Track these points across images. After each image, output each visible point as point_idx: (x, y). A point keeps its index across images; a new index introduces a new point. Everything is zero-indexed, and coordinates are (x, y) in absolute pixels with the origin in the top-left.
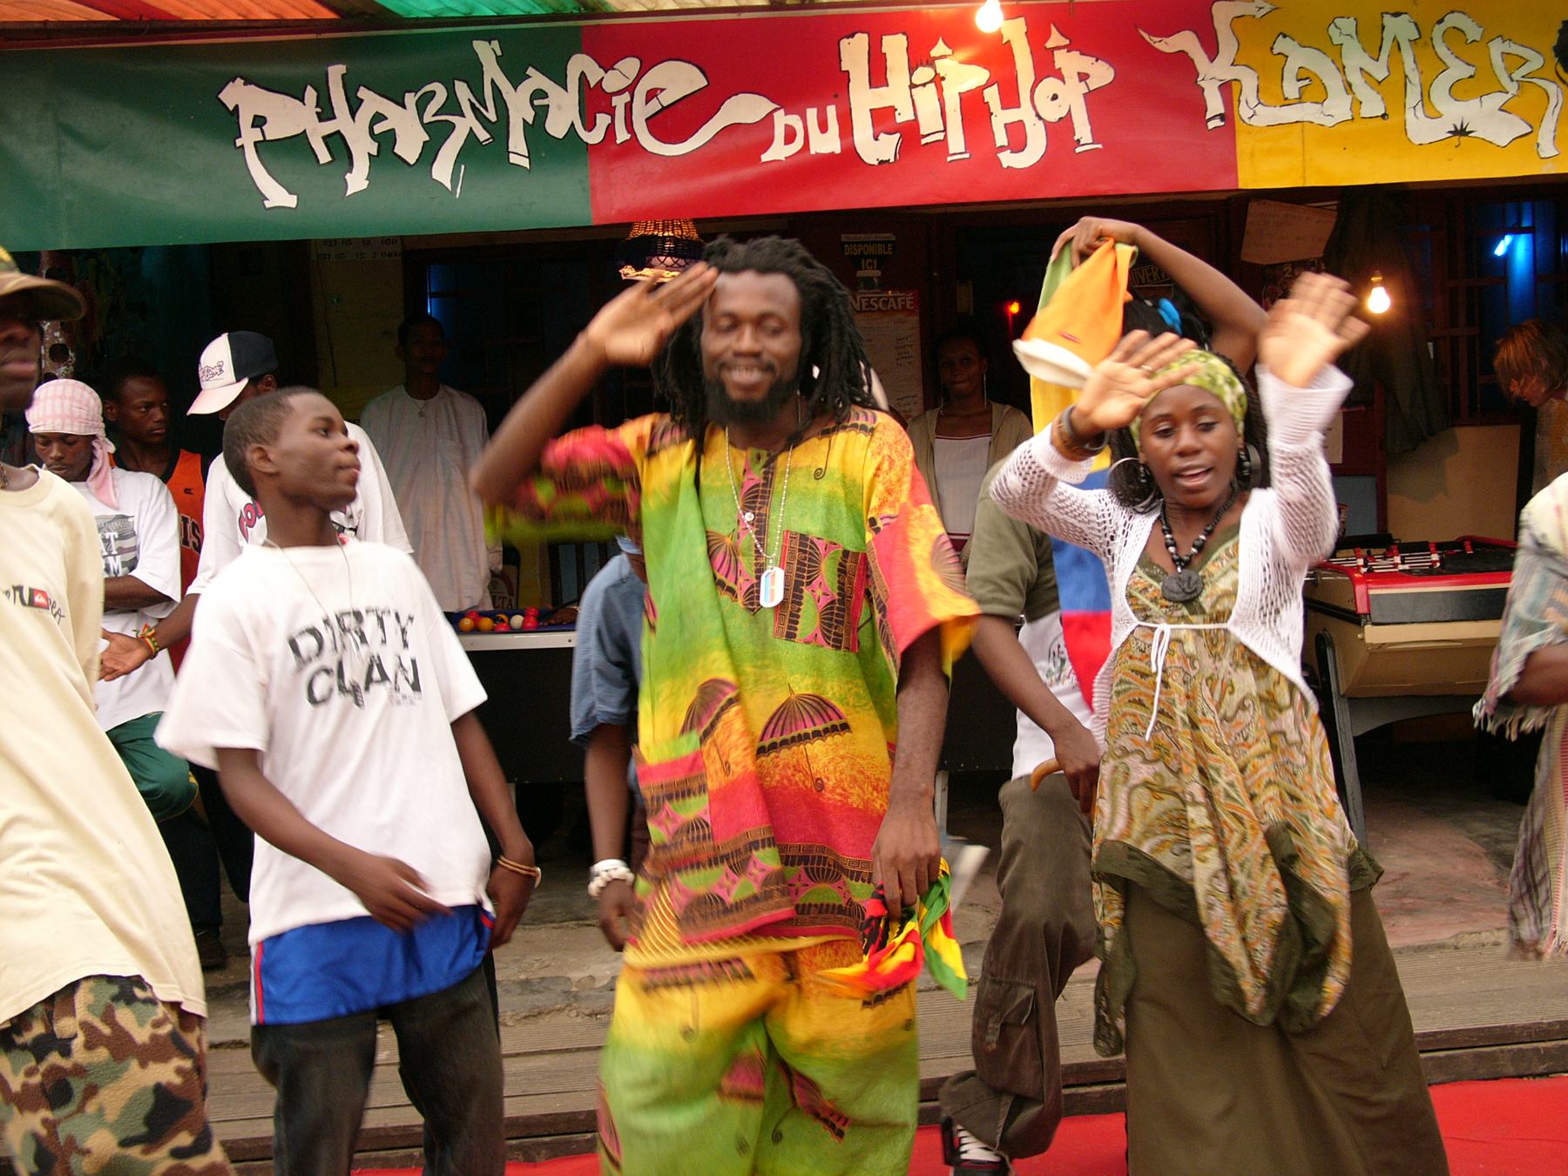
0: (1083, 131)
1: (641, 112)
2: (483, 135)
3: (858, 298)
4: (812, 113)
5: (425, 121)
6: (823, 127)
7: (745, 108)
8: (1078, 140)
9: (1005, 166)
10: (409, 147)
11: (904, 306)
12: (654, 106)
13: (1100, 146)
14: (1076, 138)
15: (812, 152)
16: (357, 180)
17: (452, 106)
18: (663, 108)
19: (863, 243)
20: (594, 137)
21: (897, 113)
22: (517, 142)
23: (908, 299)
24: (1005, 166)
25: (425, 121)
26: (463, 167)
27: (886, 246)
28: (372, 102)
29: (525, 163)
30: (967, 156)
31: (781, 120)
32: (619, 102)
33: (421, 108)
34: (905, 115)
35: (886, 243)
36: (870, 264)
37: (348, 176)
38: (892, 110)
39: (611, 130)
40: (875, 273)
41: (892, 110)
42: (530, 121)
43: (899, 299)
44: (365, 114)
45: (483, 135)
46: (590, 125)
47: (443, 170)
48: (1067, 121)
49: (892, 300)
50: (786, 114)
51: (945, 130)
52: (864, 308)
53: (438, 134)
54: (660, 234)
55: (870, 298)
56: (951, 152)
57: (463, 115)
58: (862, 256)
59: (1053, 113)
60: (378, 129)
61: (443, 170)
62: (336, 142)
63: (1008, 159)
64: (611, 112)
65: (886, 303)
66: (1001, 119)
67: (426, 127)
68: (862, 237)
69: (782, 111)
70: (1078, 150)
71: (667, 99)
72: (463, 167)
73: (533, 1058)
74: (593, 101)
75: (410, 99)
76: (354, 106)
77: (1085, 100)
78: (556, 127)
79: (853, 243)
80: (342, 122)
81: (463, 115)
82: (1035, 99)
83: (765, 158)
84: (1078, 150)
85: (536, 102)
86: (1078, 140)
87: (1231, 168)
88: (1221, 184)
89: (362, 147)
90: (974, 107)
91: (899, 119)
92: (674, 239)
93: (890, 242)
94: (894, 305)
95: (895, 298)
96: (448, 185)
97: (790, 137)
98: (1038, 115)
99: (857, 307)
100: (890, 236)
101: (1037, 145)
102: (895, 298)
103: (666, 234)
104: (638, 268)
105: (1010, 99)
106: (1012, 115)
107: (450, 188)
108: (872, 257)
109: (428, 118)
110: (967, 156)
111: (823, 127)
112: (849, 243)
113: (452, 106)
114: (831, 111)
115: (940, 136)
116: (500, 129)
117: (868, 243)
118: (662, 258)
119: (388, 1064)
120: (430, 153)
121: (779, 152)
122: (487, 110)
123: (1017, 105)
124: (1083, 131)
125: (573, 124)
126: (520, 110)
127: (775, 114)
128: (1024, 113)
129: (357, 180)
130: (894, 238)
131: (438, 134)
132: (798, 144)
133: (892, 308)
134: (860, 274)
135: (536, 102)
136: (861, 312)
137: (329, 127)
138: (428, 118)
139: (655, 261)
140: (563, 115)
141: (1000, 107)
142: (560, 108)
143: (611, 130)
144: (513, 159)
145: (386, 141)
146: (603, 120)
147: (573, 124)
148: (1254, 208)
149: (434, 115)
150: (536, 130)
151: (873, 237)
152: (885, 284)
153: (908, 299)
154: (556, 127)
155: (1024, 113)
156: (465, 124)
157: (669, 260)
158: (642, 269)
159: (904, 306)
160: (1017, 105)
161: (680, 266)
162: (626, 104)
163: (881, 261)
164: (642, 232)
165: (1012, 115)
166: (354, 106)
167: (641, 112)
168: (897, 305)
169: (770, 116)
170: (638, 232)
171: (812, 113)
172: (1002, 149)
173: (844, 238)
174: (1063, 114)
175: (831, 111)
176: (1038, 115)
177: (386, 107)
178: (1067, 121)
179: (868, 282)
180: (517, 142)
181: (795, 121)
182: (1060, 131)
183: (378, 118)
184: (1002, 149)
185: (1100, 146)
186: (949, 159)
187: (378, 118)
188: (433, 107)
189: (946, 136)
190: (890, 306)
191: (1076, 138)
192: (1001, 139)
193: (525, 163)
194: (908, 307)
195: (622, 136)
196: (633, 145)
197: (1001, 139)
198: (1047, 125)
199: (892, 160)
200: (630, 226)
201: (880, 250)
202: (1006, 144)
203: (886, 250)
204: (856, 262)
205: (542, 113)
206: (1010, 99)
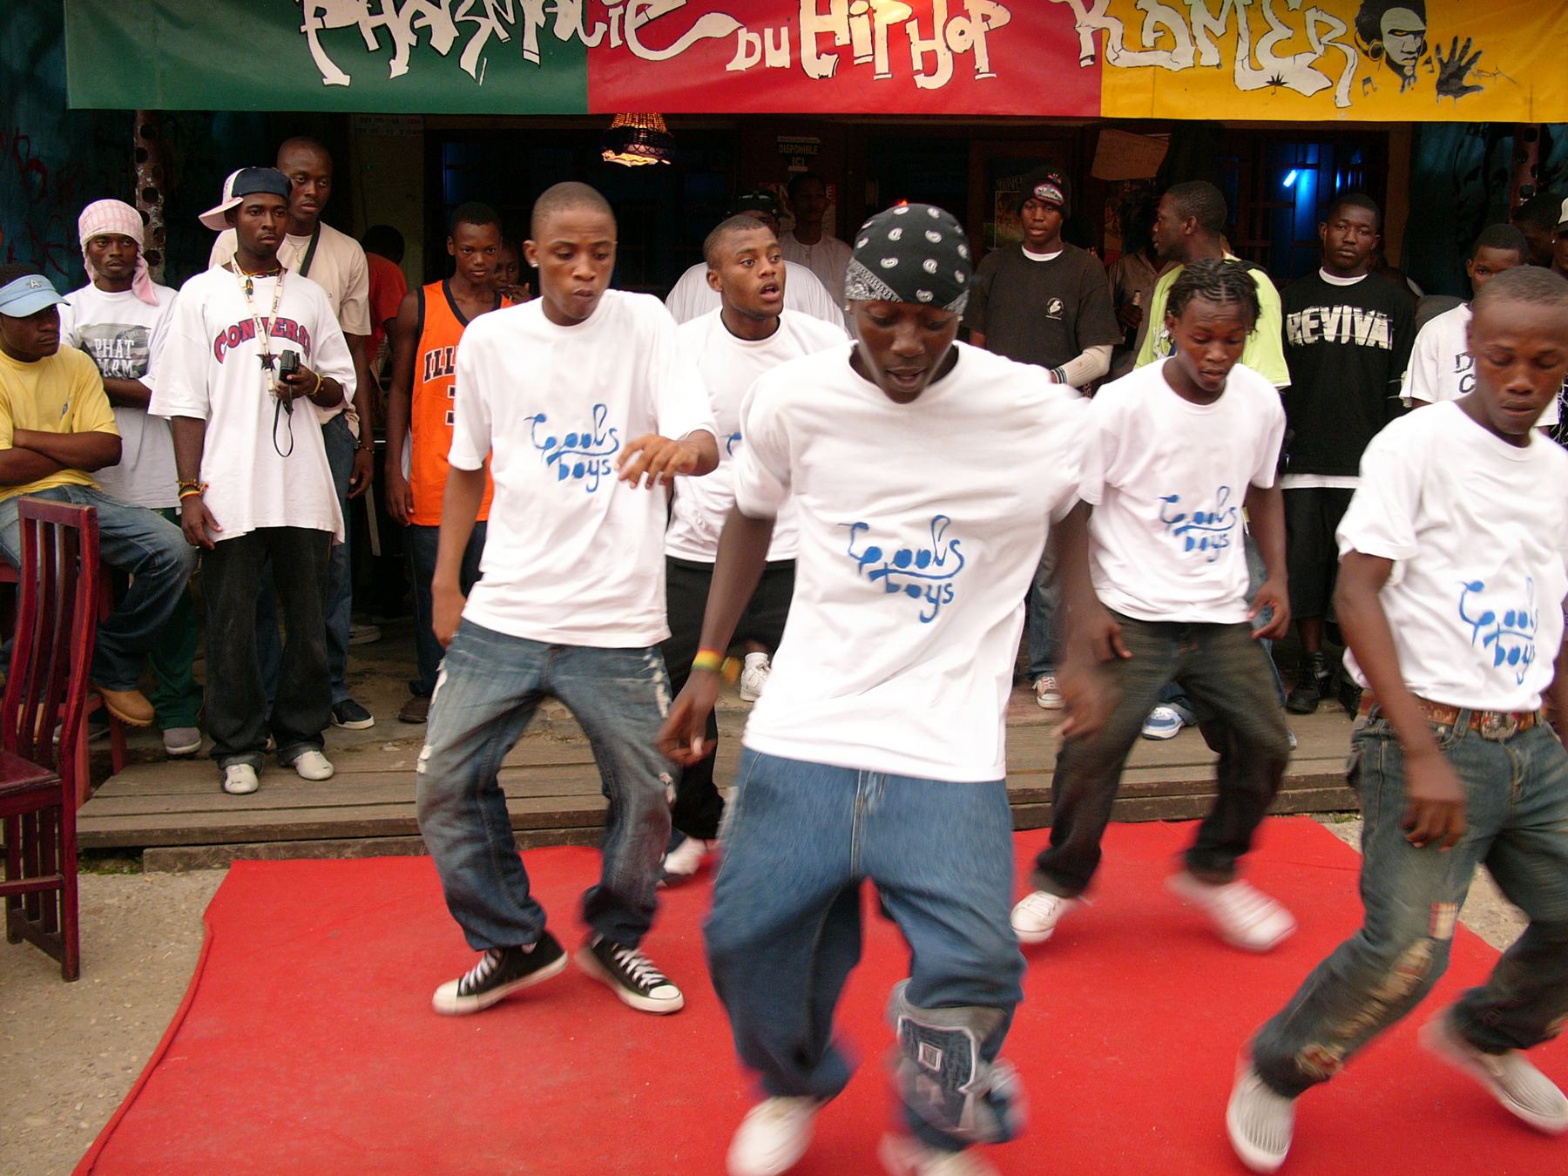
19: (794, 144)
36: (799, 162)
54: (637, 126)
68: (793, 139)
73: (517, 771)
79: (786, 143)
87: (1096, 99)
88: (1088, 112)
92: (647, 131)
93: (815, 144)
103: (641, 127)
104: (618, 153)
112: (783, 143)
117: (798, 144)
118: (637, 146)
119: (404, 771)
130: (819, 141)
134: (791, 168)
139: (631, 148)
148: (1104, 135)
151: (802, 139)
157: (642, 148)
158: (620, 154)
161: (651, 153)
164: (622, 124)
170: (618, 123)
173: (779, 139)
194: (827, 196)
200: (611, 117)
203: (813, 150)
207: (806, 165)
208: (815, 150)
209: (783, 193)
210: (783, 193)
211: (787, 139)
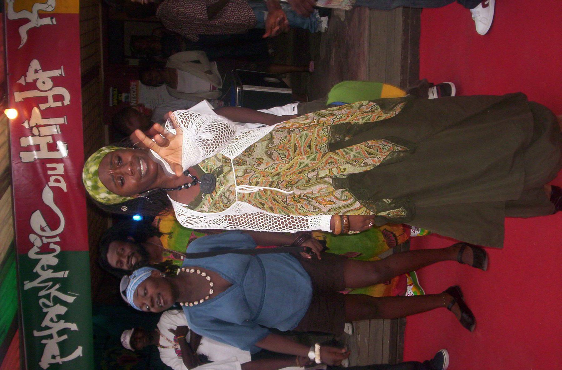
0: (57, 73)
1: (49, 233)
2: (57, 286)
3: (132, 101)
4: (50, 172)
5: (52, 305)
6: (54, 169)
7: (48, 197)
8: (60, 75)
9: (69, 103)
10: (62, 310)
11: (135, 86)
12: (47, 229)
13: (62, 67)
14: (59, 76)
15: (63, 174)
16: (73, 327)
17: (48, 297)
18: (48, 225)
19: (113, 99)
20: (58, 249)
21: (49, 142)
22: (60, 275)
23: (133, 84)
24: (69, 103)
25: (52, 305)
26: (69, 293)
27: (114, 90)
28: (46, 322)
29: (67, 272)
30: (65, 117)
31: (52, 183)
32: (45, 241)
33: (48, 306)
34: (50, 140)
35: (113, 90)
37: (72, 329)
38: (48, 144)
39: (55, 243)
40: (124, 95)
41: (48, 144)
42: (52, 271)
43: (133, 87)
44: (50, 324)
45: (57, 286)
46: (54, 250)
47: (70, 299)
48: (53, 79)
49: (133, 90)
50: (50, 182)
51: (56, 125)
52: (135, 100)
53: (57, 301)
55: (132, 97)
56: (64, 123)
57: (50, 293)
58: (117, 99)
59: (50, 84)
60: (55, 320)
61: (70, 299)
62: (61, 333)
63: (67, 102)
64: (49, 243)
65: (134, 92)
66: (52, 104)
67: (55, 304)
69: (49, 183)
70: (63, 75)
71: (44, 224)
72: (69, 293)
74: (45, 249)
75: (45, 310)
76: (47, 328)
77: (46, 71)
78: (54, 261)
80: (54, 331)
81: (50, 293)
82: (46, 90)
83: (65, 190)
84: (63, 75)
85: (46, 269)
86: (60, 75)
89: (62, 325)
90: (46, 114)
91: (52, 142)
94: (135, 89)
95: (133, 88)
96: (75, 298)
97: (57, 181)
98: (51, 89)
99: (135, 102)
100: (111, 89)
101: (62, 91)
102: (133, 88)
105: (45, 100)
106: (51, 99)
107: (75, 298)
108: (118, 96)
109: (51, 304)
110: (65, 117)
111: (54, 169)
112: (113, 104)
113: (48, 297)
114: (49, 165)
115: (58, 126)
116: (55, 281)
120: (64, 303)
121: (63, 185)
122: (48, 285)
123: (47, 96)
124: (57, 73)
125: (54, 256)
126: (49, 274)
127: (50, 186)
128: (50, 95)
129: (73, 327)
131: (57, 301)
132: (61, 178)
133: (136, 90)
135: (46, 269)
136: (137, 101)
137: (55, 336)
138: (51, 304)
140: (51, 259)
141: (47, 104)
142: (48, 261)
143: (55, 243)
144: (66, 276)
145: (60, 317)
146: (52, 246)
147: (54, 256)
149: (50, 302)
150: (56, 269)
152: (128, 91)
153: (133, 84)
154: (54, 261)
155: (50, 95)
156: (54, 292)
159: (135, 86)
160: (47, 96)
162: (46, 238)
163: (120, 93)
165: (51, 99)
166: (47, 328)
167: (49, 233)
168: (135, 88)
169: (52, 188)
171: (50, 172)
172: (63, 103)
173: (111, 105)
174: (50, 80)
175: (49, 165)
176: (51, 89)
177: (48, 318)
178: (53, 79)
179: (127, 98)
180: (60, 275)
181: (52, 179)
182: (57, 82)
183: (52, 320)
184: (63, 103)
185: (62, 67)
186: (66, 124)
187: (52, 320)
188: (48, 303)
189: (58, 124)
190: (135, 91)
191: (59, 76)
192: (59, 104)
193: (67, 272)
194: (136, 84)
195: (58, 239)
196: (60, 235)
197: (59, 104)
198: (55, 85)
199: (66, 145)
201: (116, 93)
202: (61, 102)
204: (119, 102)
205: (49, 267)
206: (45, 100)
207: (122, 94)
208: (115, 89)
209: (134, 104)
210: (134, 104)
211: (111, 102)
